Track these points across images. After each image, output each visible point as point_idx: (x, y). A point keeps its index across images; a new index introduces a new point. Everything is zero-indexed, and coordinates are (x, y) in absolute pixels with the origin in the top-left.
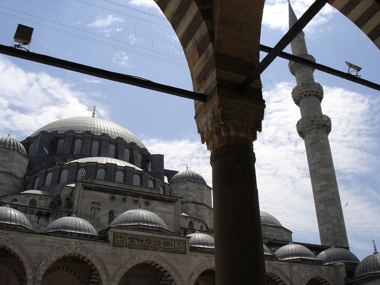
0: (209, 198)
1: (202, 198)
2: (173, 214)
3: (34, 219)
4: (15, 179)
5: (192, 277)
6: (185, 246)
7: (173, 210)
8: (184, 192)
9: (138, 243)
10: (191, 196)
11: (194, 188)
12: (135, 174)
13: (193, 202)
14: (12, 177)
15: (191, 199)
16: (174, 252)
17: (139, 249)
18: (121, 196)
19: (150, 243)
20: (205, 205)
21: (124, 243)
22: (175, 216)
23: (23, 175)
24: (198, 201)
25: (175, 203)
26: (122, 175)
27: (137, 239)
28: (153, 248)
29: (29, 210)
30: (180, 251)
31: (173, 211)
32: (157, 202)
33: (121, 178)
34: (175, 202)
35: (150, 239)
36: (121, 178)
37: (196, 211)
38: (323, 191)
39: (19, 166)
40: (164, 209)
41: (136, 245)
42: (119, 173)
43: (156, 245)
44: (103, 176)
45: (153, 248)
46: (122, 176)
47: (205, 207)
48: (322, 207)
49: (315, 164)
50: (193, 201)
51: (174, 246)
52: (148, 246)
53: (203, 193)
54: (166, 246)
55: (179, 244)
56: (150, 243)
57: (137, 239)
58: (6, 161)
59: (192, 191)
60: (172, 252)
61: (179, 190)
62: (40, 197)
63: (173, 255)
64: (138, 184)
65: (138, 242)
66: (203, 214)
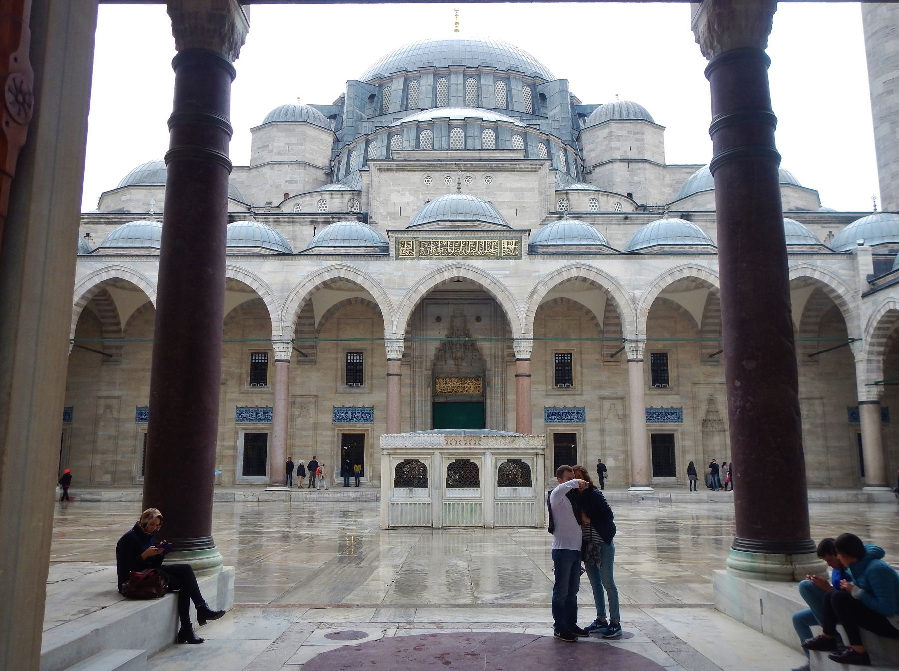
0: (657, 147)
1: (641, 150)
2: (536, 192)
3: (307, 233)
4: (313, 170)
5: (535, 297)
6: (521, 246)
7: (536, 185)
8: (606, 143)
9: (436, 250)
10: (619, 149)
11: (624, 133)
12: (483, 129)
13: (622, 161)
14: (307, 168)
15: (617, 155)
16: (500, 258)
17: (438, 259)
18: (442, 173)
19: (457, 249)
20: (646, 161)
21: (414, 253)
22: (541, 193)
23: (326, 162)
24: (632, 155)
25: (540, 171)
26: (461, 135)
27: (435, 244)
28: (464, 255)
29: (297, 220)
30: (512, 256)
31: (537, 186)
32: (507, 174)
33: (461, 140)
34: (540, 168)
35: (457, 242)
36: (461, 140)
37: (628, 176)
38: (890, 92)
39: (316, 148)
40: (517, 185)
41: (434, 255)
42: (456, 132)
43: (468, 249)
44: (429, 141)
45: (464, 255)
46: (462, 137)
47: (647, 165)
48: (885, 128)
49: (874, 34)
50: (622, 158)
51: (501, 248)
52: (454, 253)
53: (642, 140)
54: (485, 250)
55: (509, 244)
56: (457, 249)
57: (435, 244)
58: (294, 144)
59: (619, 138)
60: (497, 259)
61: (597, 141)
62: (332, 194)
63: (499, 264)
64: (493, 147)
65: (436, 248)
66: (643, 179)
